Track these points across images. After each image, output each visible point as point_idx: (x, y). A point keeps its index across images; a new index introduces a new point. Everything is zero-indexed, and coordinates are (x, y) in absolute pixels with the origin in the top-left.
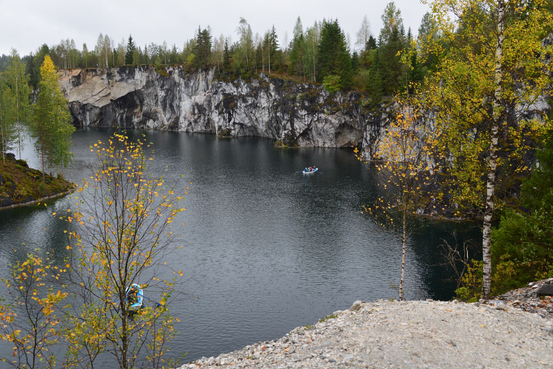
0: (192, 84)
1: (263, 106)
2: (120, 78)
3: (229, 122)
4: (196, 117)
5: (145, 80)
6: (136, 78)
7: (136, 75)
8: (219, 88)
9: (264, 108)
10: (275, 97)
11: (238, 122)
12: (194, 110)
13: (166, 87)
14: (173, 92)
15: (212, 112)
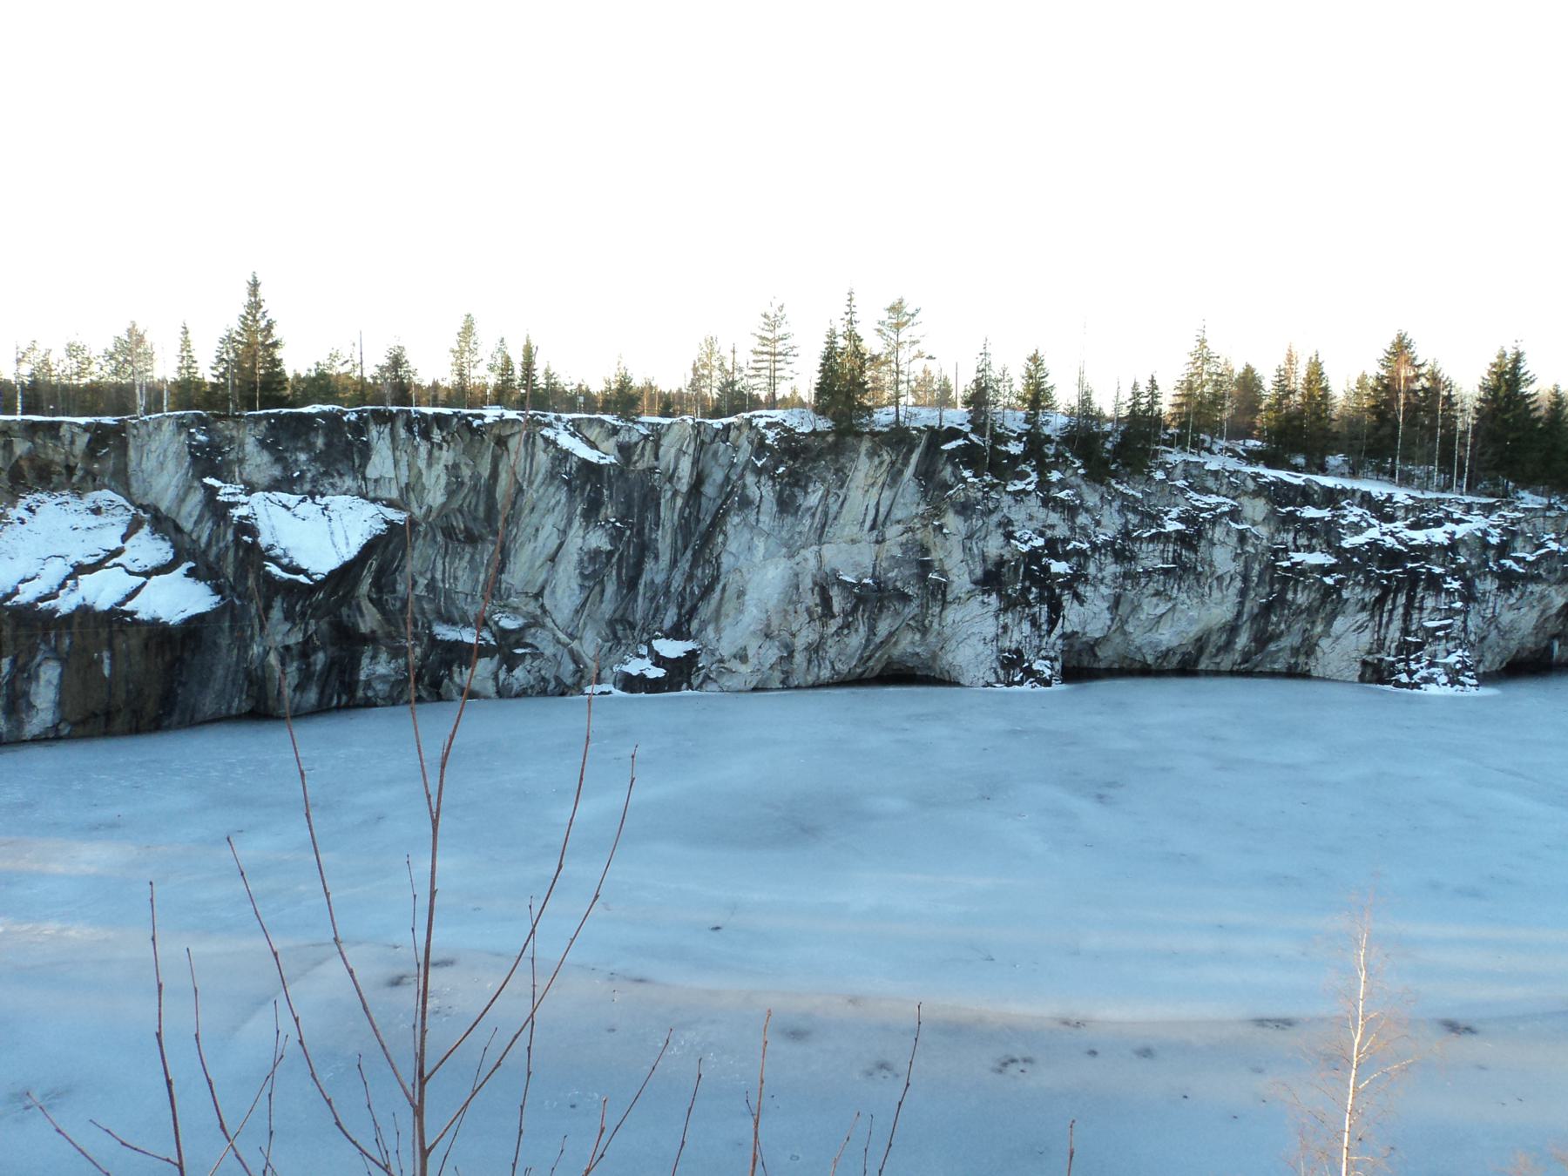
0: (813, 499)
1: (1220, 572)
2: (277, 471)
3: (1050, 632)
4: (833, 625)
5: (443, 480)
6: (371, 472)
7: (375, 459)
8: (991, 512)
9: (1220, 579)
10: (1271, 538)
11: (1068, 629)
12: (826, 601)
13: (609, 512)
14: (640, 533)
15: (945, 604)
